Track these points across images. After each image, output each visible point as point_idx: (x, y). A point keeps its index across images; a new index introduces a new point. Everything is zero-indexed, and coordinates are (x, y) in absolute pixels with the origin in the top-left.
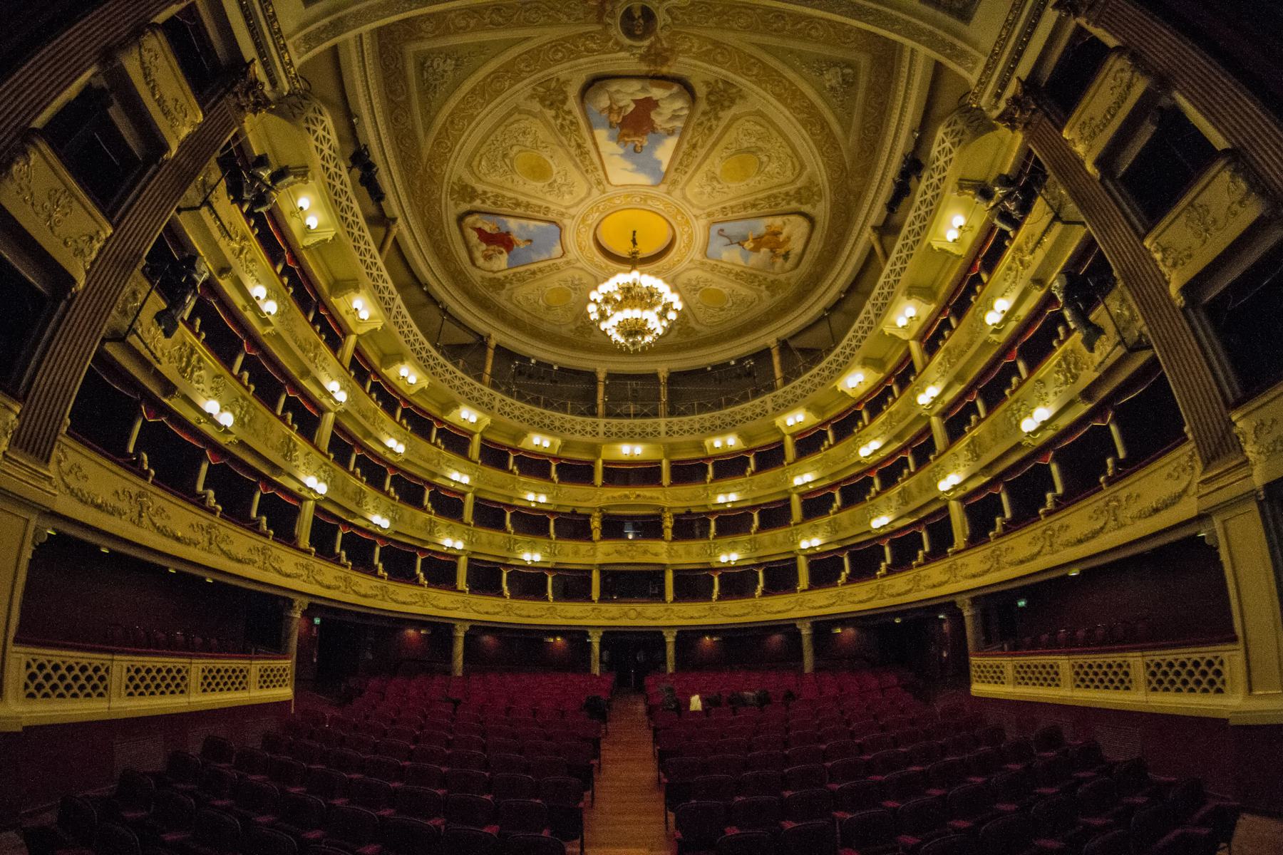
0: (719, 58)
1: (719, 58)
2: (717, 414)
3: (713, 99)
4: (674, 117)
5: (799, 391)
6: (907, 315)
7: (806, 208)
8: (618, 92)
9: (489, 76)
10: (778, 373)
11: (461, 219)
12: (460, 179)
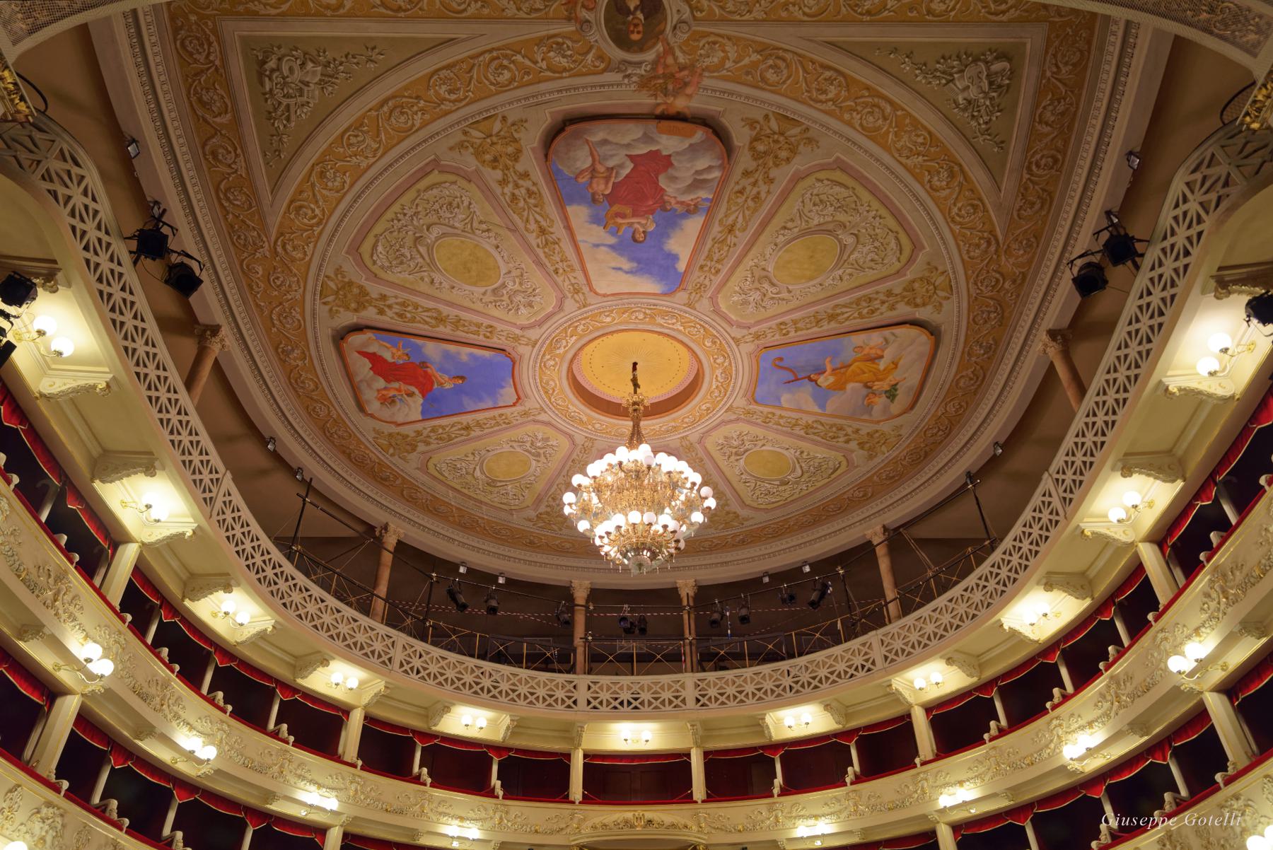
0: (771, 75)
1: (771, 75)
2: (784, 665)
3: (761, 147)
4: (697, 184)
5: (930, 628)
6: (1127, 504)
7: (922, 314)
9: (385, 101)
10: (890, 593)
11: (340, 337)
12: (338, 271)
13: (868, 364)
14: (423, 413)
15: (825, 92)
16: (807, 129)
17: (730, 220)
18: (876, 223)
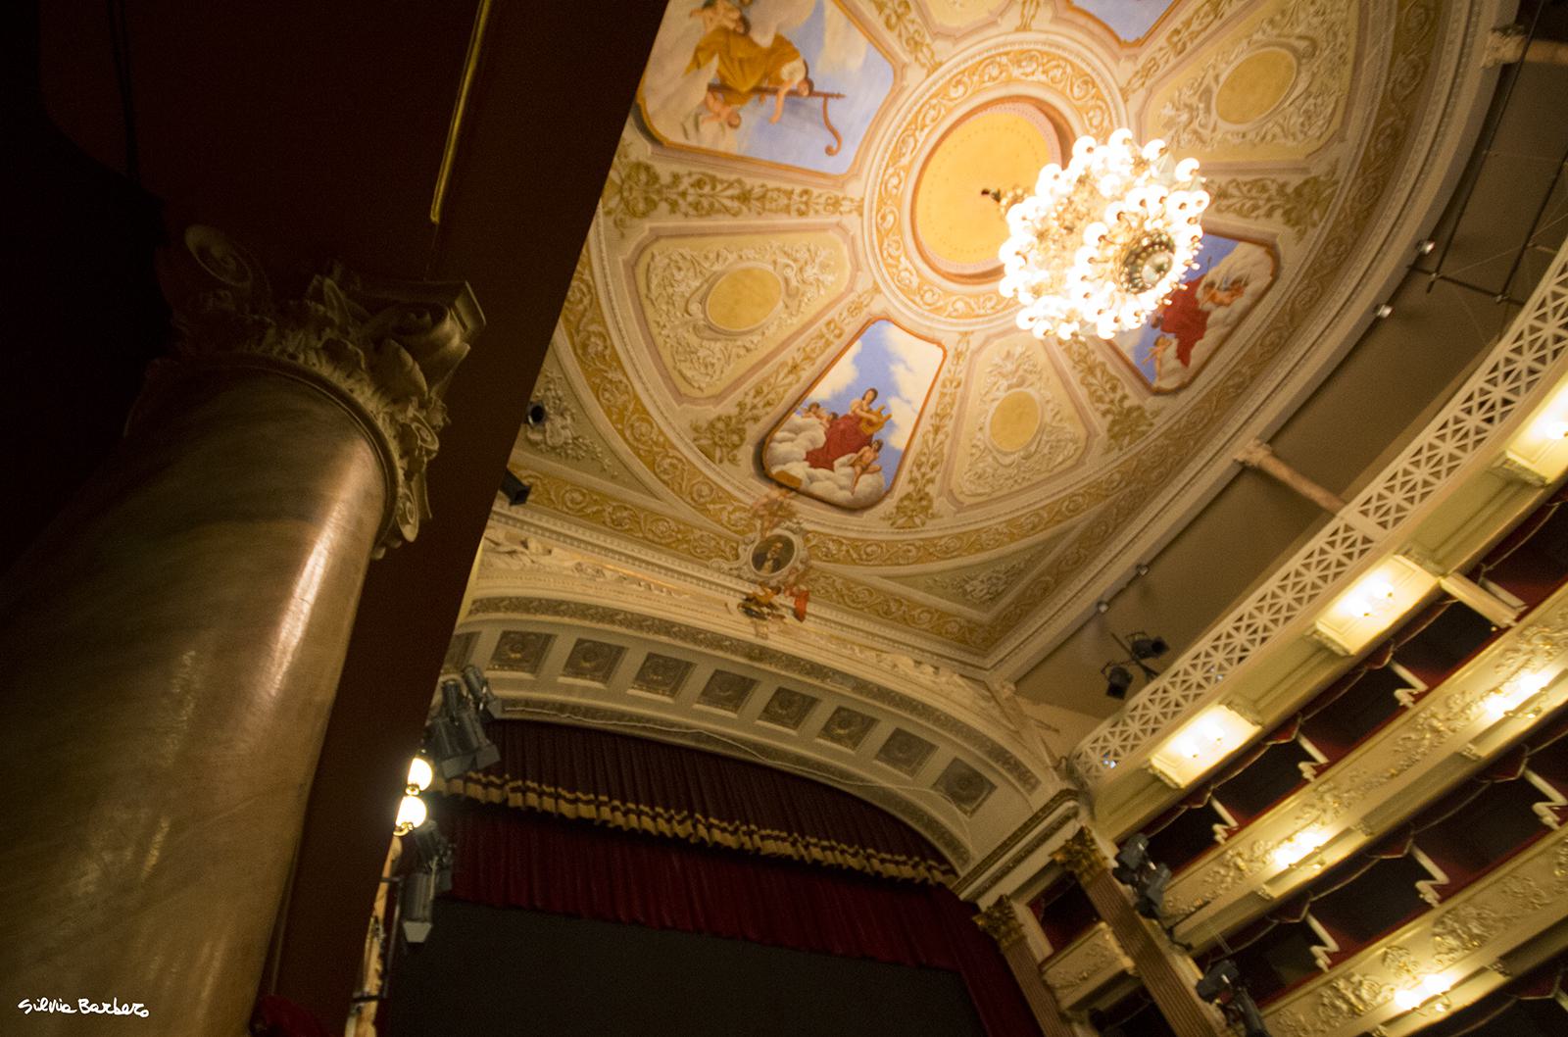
0: (705, 490)
1: (705, 490)
3: (735, 438)
4: (797, 430)
8: (842, 488)
9: (953, 557)
12: (1108, 450)
13: (730, 83)
14: (1228, 252)
15: (671, 465)
16: (695, 440)
17: (791, 377)
18: (663, 320)
